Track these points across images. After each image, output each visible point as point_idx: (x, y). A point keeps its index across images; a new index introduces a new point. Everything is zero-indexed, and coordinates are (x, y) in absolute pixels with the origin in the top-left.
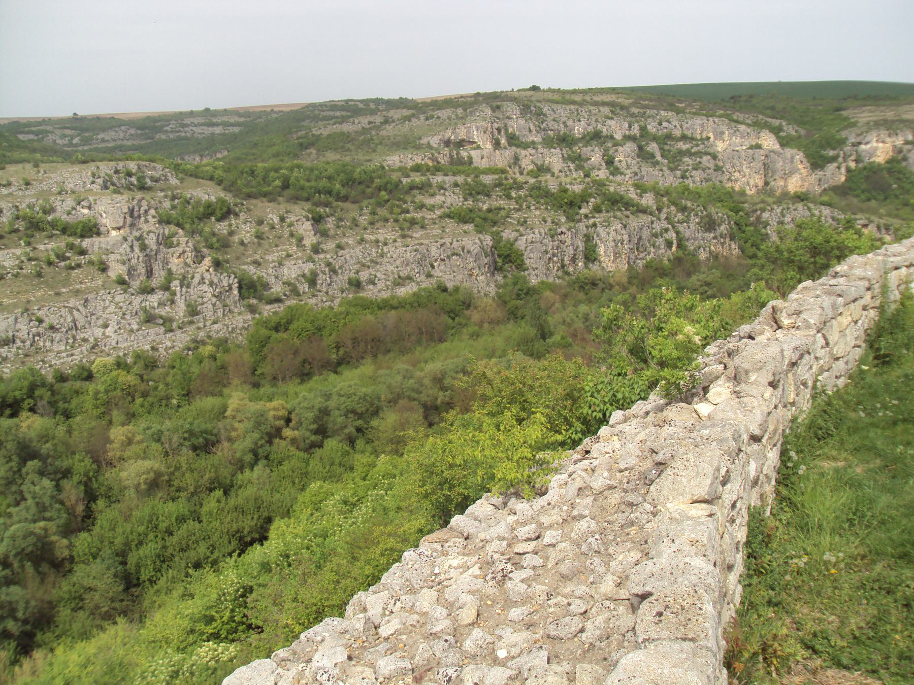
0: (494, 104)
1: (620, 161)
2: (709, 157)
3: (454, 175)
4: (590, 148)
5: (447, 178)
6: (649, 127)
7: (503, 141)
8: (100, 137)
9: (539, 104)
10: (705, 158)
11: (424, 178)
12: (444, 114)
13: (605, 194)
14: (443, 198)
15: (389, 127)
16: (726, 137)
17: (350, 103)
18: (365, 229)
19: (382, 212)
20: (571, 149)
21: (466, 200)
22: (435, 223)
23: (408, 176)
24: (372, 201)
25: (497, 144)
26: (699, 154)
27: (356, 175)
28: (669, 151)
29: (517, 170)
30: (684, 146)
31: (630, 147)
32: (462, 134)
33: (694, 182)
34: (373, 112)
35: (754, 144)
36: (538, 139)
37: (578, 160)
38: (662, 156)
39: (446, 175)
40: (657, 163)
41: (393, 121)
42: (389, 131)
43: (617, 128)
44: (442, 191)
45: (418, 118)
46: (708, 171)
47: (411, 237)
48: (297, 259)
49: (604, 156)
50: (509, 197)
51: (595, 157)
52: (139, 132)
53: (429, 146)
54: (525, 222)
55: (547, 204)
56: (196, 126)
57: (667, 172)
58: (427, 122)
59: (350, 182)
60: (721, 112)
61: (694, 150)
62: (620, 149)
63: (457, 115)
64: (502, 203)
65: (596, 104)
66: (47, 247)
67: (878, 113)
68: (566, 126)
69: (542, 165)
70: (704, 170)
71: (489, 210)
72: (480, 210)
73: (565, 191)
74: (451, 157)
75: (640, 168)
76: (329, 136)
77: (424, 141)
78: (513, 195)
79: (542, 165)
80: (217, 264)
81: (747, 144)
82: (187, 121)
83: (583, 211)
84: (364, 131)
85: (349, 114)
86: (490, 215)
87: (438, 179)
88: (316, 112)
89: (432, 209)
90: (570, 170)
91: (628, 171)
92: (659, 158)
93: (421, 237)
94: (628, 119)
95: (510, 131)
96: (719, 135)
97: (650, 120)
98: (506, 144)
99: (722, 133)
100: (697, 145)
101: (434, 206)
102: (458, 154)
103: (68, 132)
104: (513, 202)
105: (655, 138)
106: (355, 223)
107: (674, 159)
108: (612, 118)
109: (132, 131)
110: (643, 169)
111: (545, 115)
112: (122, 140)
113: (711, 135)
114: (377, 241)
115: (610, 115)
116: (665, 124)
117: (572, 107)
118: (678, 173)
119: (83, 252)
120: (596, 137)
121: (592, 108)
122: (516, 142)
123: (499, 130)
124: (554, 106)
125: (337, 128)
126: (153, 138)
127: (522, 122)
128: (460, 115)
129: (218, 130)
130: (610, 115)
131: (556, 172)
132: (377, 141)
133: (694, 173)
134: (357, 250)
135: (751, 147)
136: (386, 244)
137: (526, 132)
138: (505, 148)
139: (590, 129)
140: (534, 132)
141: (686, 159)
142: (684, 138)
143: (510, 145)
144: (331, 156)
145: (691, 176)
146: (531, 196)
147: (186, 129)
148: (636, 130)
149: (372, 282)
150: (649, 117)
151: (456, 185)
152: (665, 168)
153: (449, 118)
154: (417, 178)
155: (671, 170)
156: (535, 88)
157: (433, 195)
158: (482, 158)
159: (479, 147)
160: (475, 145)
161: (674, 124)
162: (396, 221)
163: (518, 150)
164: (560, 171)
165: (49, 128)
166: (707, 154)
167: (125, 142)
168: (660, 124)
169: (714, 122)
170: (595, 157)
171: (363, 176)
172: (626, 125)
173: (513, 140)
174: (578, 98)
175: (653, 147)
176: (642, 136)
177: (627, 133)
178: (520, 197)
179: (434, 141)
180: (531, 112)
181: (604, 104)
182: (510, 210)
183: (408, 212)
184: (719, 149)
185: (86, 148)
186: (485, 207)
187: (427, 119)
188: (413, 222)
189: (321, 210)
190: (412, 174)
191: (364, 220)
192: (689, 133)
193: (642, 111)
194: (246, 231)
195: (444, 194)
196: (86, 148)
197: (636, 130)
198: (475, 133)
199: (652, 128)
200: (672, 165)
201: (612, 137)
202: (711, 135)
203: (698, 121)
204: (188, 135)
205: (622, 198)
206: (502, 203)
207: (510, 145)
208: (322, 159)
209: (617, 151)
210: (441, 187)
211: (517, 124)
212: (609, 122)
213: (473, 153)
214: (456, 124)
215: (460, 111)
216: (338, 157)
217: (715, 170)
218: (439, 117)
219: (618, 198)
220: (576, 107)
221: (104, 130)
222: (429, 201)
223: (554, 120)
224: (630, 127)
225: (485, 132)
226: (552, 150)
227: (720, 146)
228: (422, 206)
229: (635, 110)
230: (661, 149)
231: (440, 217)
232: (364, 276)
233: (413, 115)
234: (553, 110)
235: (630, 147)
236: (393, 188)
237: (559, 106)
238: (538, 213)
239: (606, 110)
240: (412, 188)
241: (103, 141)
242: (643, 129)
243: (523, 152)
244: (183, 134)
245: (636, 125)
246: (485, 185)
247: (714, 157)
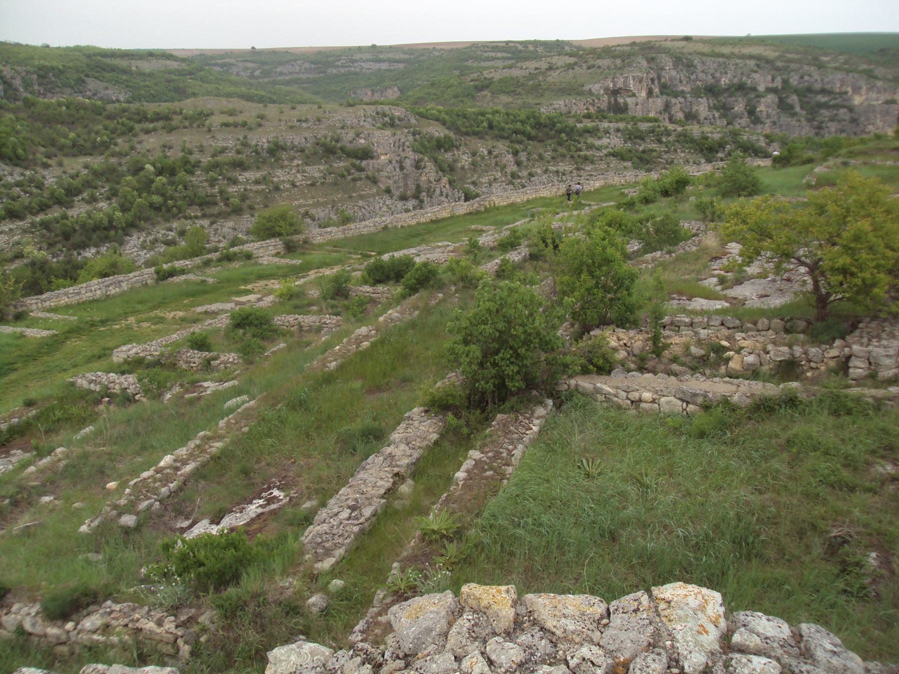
0: (650, 56)
1: (761, 111)
2: (845, 110)
4: (733, 99)
5: (612, 125)
6: (791, 80)
7: (656, 90)
8: (279, 70)
9: (689, 57)
10: (842, 111)
11: (594, 124)
12: (605, 62)
13: (739, 142)
14: (608, 141)
15: (555, 74)
16: (863, 91)
17: (510, 44)
18: (548, 162)
19: (562, 150)
20: (717, 98)
21: (626, 142)
23: (581, 122)
24: (554, 140)
25: (650, 93)
26: (836, 107)
27: (542, 121)
28: (808, 103)
29: (666, 116)
30: (822, 99)
31: (771, 98)
32: (620, 84)
33: (829, 133)
35: (890, 98)
36: (687, 89)
37: (725, 109)
38: (802, 108)
39: (611, 122)
41: (557, 68)
43: (762, 80)
45: (581, 66)
46: (844, 123)
48: (502, 182)
49: (746, 106)
50: (660, 141)
51: (739, 107)
52: (313, 66)
53: (590, 92)
54: (672, 162)
55: (690, 148)
56: (364, 61)
57: (804, 123)
58: (589, 71)
59: (538, 125)
61: (831, 103)
62: (763, 100)
63: (615, 65)
64: (654, 146)
65: (743, 57)
66: (341, 165)
68: (714, 77)
69: (690, 113)
70: (840, 121)
71: (644, 152)
72: (637, 151)
73: (707, 138)
74: (610, 103)
75: (779, 118)
76: (501, 81)
77: (586, 88)
78: (664, 140)
79: (690, 113)
80: (451, 183)
81: (883, 97)
82: (357, 57)
83: (720, 155)
84: (532, 76)
85: (509, 55)
86: (645, 156)
88: (479, 53)
89: (599, 149)
90: (714, 118)
91: (768, 121)
92: (798, 109)
94: (773, 72)
95: (663, 80)
96: (857, 90)
97: (792, 74)
98: (659, 93)
99: (860, 88)
100: (835, 99)
101: (601, 147)
102: (616, 100)
103: (249, 65)
104: (663, 146)
105: (796, 91)
106: (541, 157)
107: (813, 111)
108: (756, 72)
109: (307, 65)
110: (782, 119)
111: (695, 67)
112: (298, 73)
113: (849, 89)
114: (557, 172)
115: (755, 69)
116: (806, 78)
117: (721, 60)
118: (815, 123)
119: (361, 170)
120: (741, 88)
121: (738, 61)
122: (668, 91)
123: (652, 80)
124: (704, 59)
126: (325, 72)
127: (674, 73)
128: (619, 66)
129: (384, 66)
130: (755, 69)
131: (702, 118)
132: (544, 87)
133: (829, 124)
134: (544, 177)
135: (887, 102)
136: (564, 174)
137: (677, 82)
138: (657, 96)
139: (736, 81)
140: (684, 82)
141: (823, 111)
142: (823, 91)
143: (662, 93)
145: (827, 127)
146: (678, 141)
147: (356, 64)
148: (778, 83)
150: (792, 71)
151: (618, 130)
152: (803, 119)
153: (609, 68)
154: (589, 124)
155: (809, 120)
157: (600, 138)
158: (637, 104)
159: (634, 95)
160: (630, 94)
161: (816, 78)
162: (572, 157)
163: (669, 98)
164: (706, 119)
165: (233, 61)
166: (843, 107)
167: (301, 76)
168: (802, 77)
169: (854, 77)
170: (739, 107)
171: (548, 121)
172: (769, 78)
173: (664, 89)
174: (726, 50)
175: (794, 99)
176: (783, 88)
177: (771, 85)
178: (669, 142)
179: (596, 88)
180: (683, 63)
181: (751, 57)
182: (661, 152)
183: (580, 150)
185: (266, 80)
186: (641, 149)
187: (589, 68)
188: (586, 158)
189: (517, 147)
190: (584, 120)
191: (548, 155)
192: (828, 87)
193: (785, 64)
194: (465, 160)
196: (266, 80)
197: (778, 83)
198: (632, 82)
199: (794, 80)
200: (810, 117)
201: (754, 89)
202: (849, 89)
203: (839, 76)
204: (358, 70)
205: (753, 145)
206: (654, 146)
207: (662, 93)
208: (496, 100)
209: (758, 102)
210: (607, 132)
211: (670, 72)
212: (754, 75)
213: (628, 100)
214: (614, 73)
215: (618, 61)
216: (511, 99)
217: (850, 122)
218: (599, 67)
219: (749, 145)
220: (725, 60)
221: (281, 64)
223: (703, 72)
224: (773, 79)
225: (640, 82)
226: (700, 99)
227: (857, 100)
228: (590, 147)
229: (779, 64)
230: (800, 101)
231: (606, 155)
233: (576, 64)
234: (703, 63)
235: (771, 98)
236: (571, 132)
237: (709, 59)
238: (683, 155)
239: (752, 63)
241: (281, 74)
242: (785, 82)
243: (673, 101)
244: (353, 69)
245: (779, 79)
246: (641, 132)
247: (851, 110)
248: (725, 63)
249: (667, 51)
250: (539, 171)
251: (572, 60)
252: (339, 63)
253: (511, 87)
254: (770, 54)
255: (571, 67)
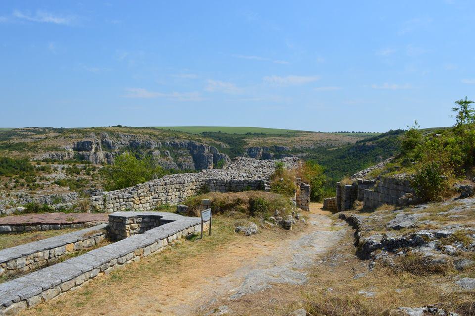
3: (63, 164)
5: (60, 166)
14: (56, 175)
17: (36, 129)
22: (49, 187)
34: (41, 133)
42: (47, 142)
44: (56, 171)
47: (35, 193)
50: (89, 174)
60: (197, 138)
64: (86, 177)
65: (143, 134)
67: (257, 140)
71: (78, 181)
101: (49, 178)
104: (90, 176)
121: (141, 135)
125: (23, 141)
132: (39, 147)
144: (15, 153)
154: (43, 164)
156: (119, 126)
157: (49, 173)
174: (135, 131)
180: (115, 136)
181: (147, 133)
190: (42, 163)
195: (57, 173)
206: (86, 177)
208: (10, 154)
210: (55, 169)
215: (81, 135)
222: (48, 176)
240: (38, 169)
248: (134, 136)
249: (107, 131)
251: (58, 134)
253: (20, 147)
254: (157, 133)
255: (56, 137)
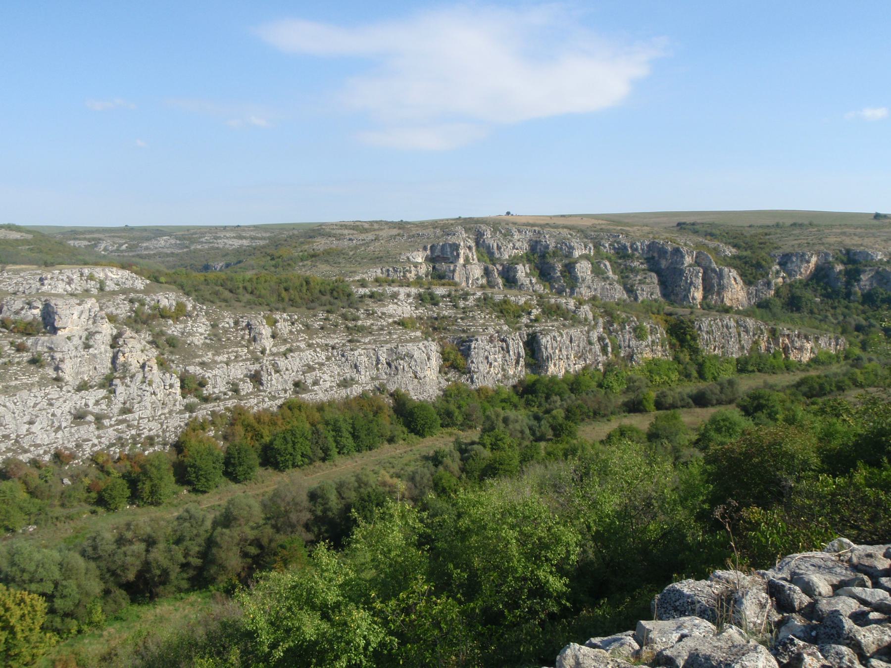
0: (468, 226)
14: (395, 306)
21: (417, 308)
34: (365, 231)
38: (614, 273)
40: (608, 278)
44: (395, 301)
48: (247, 360)
50: (455, 306)
52: (178, 242)
56: (227, 238)
87: (389, 290)
93: (369, 343)
109: (173, 241)
129: (245, 243)
144: (324, 268)
147: (219, 241)
149: (316, 383)
184: (663, 267)
195: (396, 303)
204: (221, 246)
208: (314, 269)
210: (395, 296)
221: (148, 239)
231: (389, 324)
232: (309, 379)
241: (147, 248)
244: (216, 245)
250: (303, 345)
252: (203, 240)
253: (328, 256)
